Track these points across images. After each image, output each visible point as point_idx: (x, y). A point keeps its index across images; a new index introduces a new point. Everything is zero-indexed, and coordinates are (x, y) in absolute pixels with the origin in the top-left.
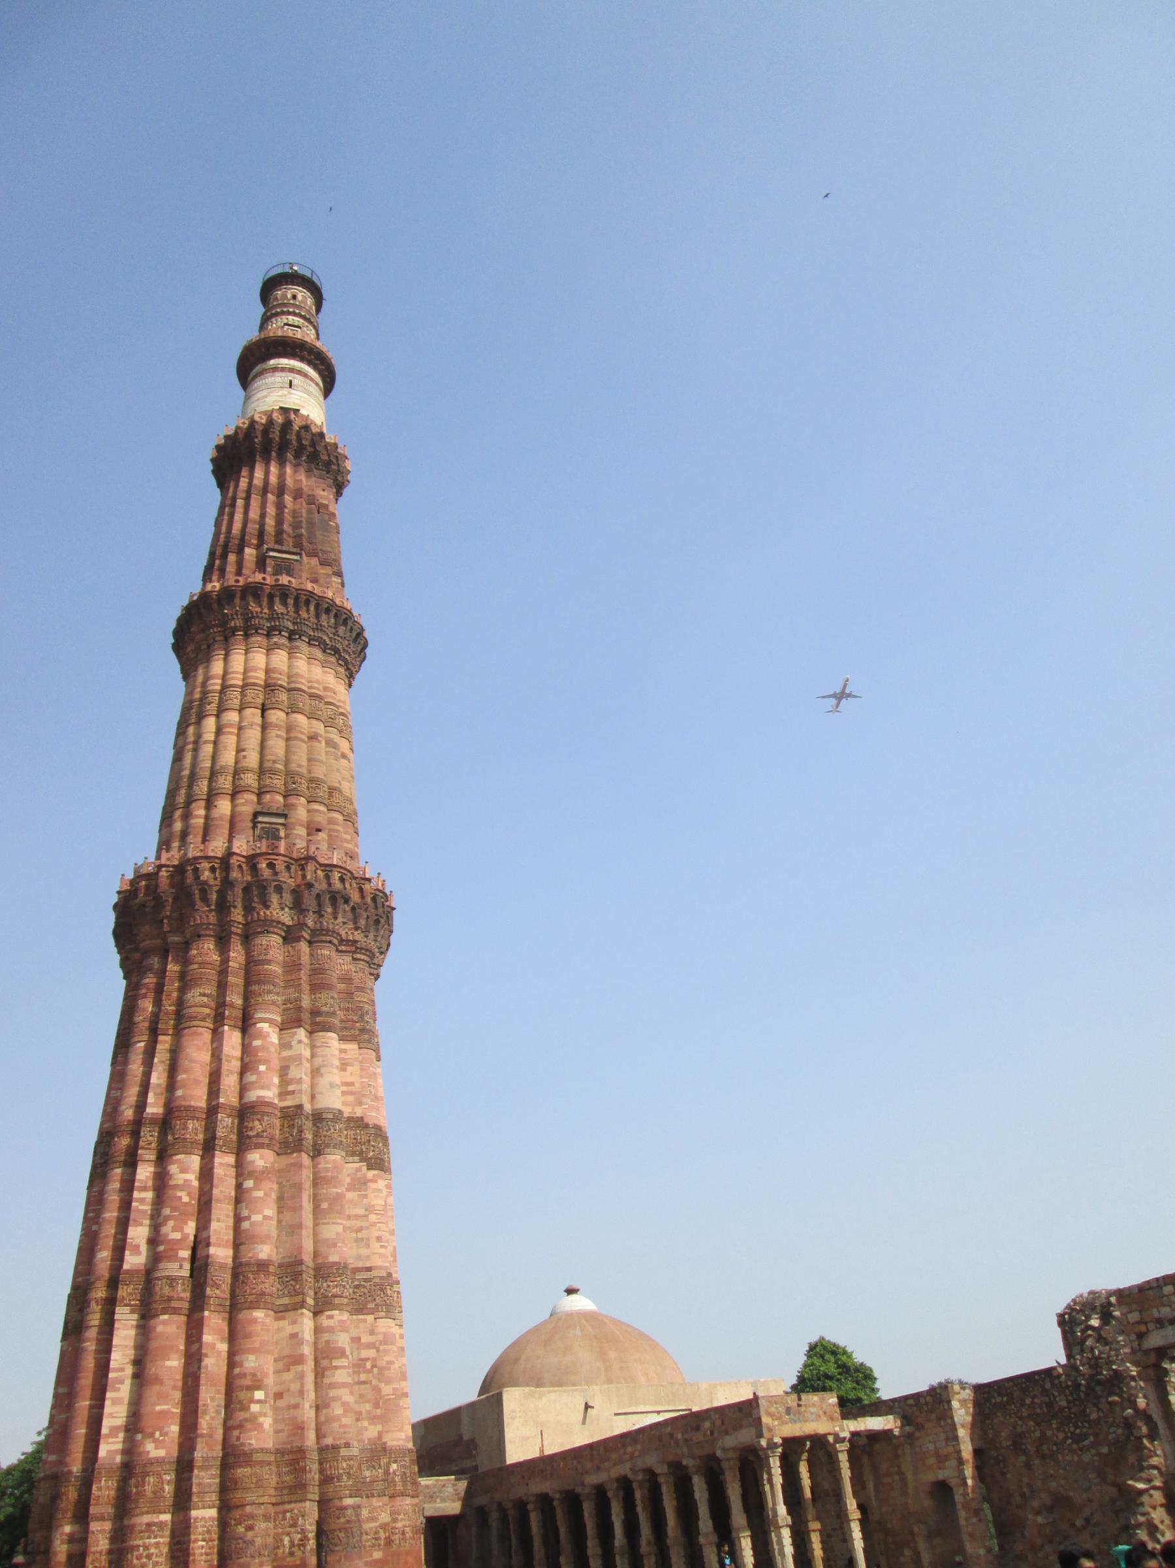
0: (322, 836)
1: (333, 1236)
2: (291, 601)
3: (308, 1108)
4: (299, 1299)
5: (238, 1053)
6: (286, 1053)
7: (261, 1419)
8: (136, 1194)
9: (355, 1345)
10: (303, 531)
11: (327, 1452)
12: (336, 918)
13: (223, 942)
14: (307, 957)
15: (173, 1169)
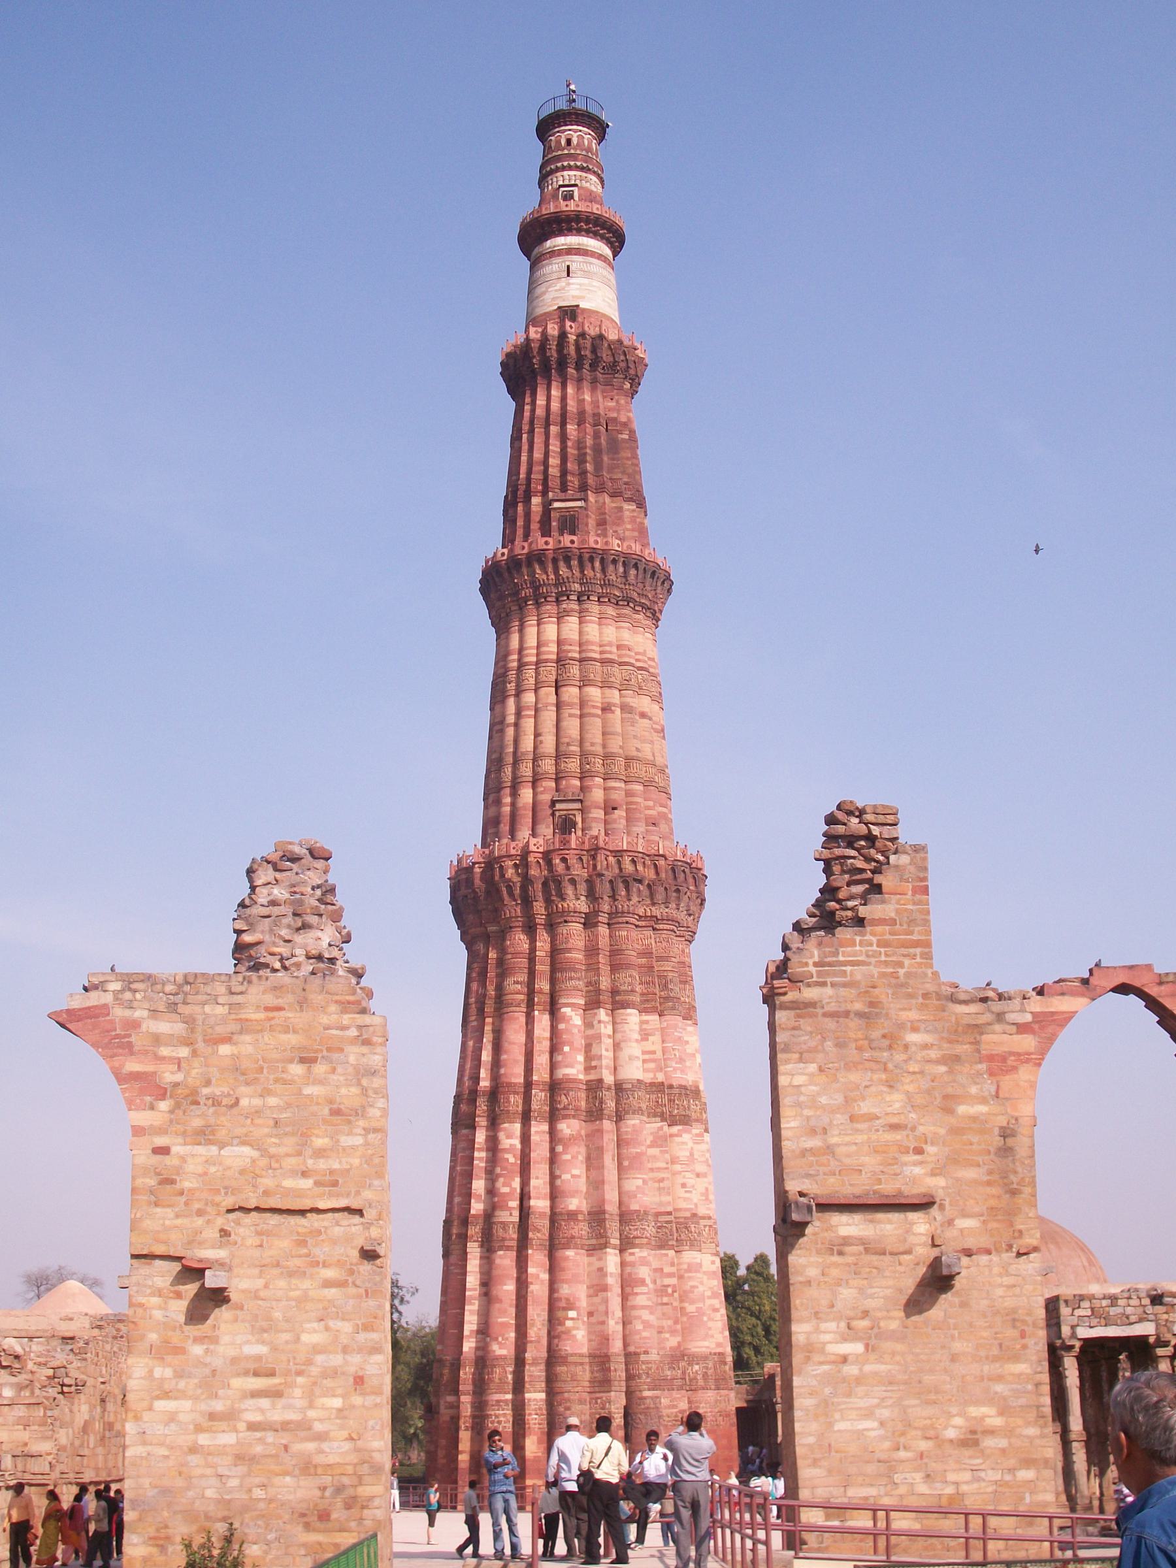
0: (620, 813)
1: (634, 1188)
2: (575, 563)
3: (609, 1079)
4: (602, 1241)
5: (548, 1035)
6: (590, 1032)
7: (574, 1332)
8: (476, 1154)
9: (658, 1274)
10: (589, 467)
11: (630, 1357)
12: (630, 900)
13: (530, 930)
14: (607, 939)
15: (501, 1135)
